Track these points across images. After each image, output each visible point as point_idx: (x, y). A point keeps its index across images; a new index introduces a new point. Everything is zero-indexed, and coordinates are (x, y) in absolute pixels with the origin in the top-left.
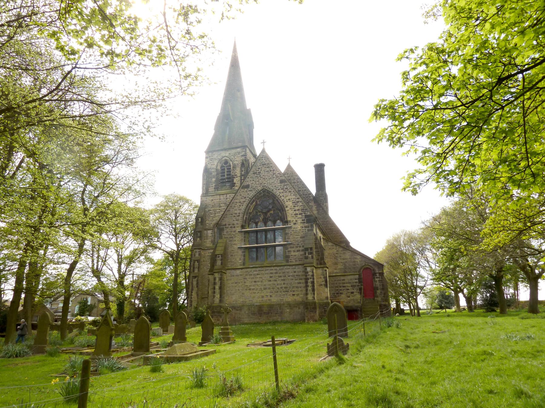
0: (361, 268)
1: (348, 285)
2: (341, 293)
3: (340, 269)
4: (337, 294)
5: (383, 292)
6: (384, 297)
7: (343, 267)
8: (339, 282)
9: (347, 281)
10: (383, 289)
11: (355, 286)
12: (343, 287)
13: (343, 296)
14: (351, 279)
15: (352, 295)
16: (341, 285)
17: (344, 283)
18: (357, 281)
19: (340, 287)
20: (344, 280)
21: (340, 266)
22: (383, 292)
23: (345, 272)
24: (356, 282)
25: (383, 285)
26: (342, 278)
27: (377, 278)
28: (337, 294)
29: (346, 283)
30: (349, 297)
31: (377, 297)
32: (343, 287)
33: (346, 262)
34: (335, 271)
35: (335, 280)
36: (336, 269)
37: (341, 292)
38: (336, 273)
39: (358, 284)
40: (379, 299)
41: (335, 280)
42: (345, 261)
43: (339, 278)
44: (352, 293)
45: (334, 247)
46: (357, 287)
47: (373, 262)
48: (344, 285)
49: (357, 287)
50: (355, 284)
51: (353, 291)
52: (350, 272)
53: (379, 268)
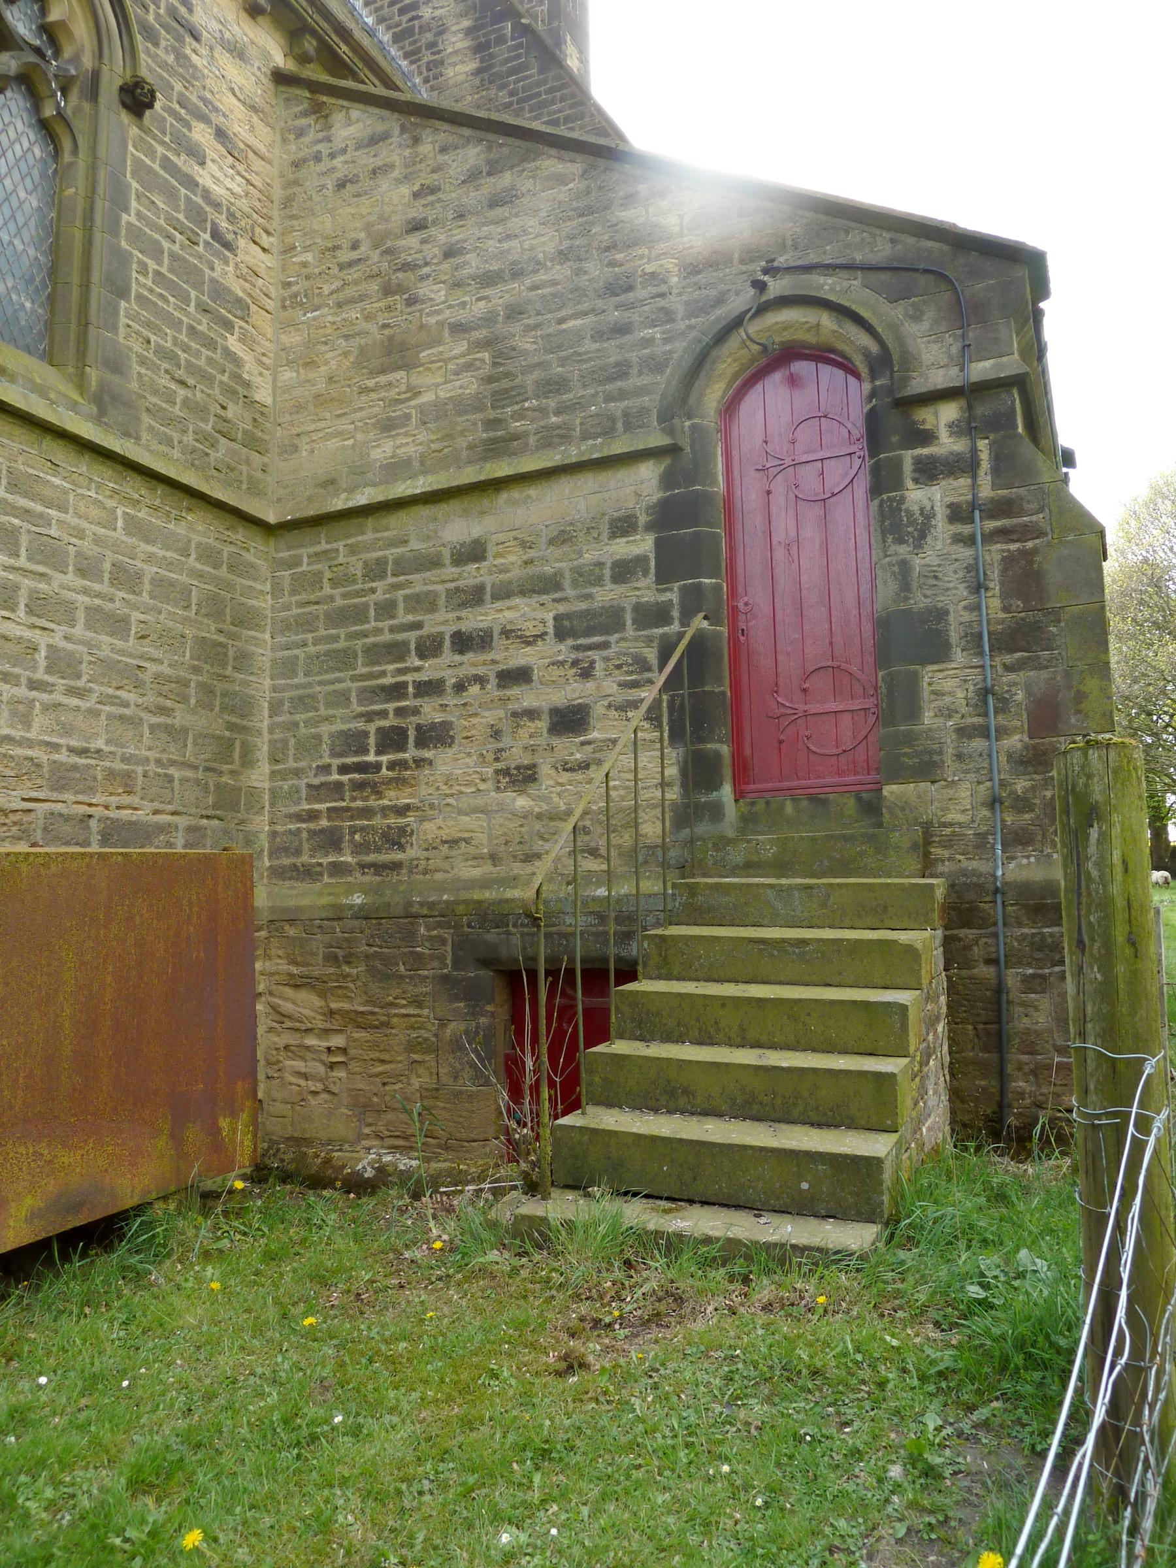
0: (700, 363)
1: (526, 613)
2: (435, 736)
3: (439, 411)
4: (392, 739)
5: (1019, 687)
6: (1035, 760)
7: (469, 385)
8: (419, 583)
9: (508, 562)
10: (1020, 639)
11: (607, 622)
12: (463, 642)
13: (448, 763)
14: (562, 538)
15: (569, 748)
16: (442, 622)
17: (475, 597)
18: (643, 545)
19: (429, 648)
20: (474, 552)
21: (445, 378)
22: (1019, 687)
23: (494, 448)
24: (624, 571)
25: (1025, 579)
26: (457, 527)
27: (928, 471)
28: (392, 739)
29: (503, 593)
30: (523, 777)
31: (927, 769)
32: (463, 642)
33: (514, 312)
34: (383, 451)
35: (376, 571)
36: (388, 426)
37: (430, 711)
38: (396, 468)
39: (645, 590)
40: (957, 801)
41: (376, 571)
42: (499, 297)
43: (415, 532)
44: (570, 720)
45: (394, 153)
46: (631, 641)
47: (882, 249)
48: (474, 620)
49: (631, 641)
50: (607, 594)
51: (573, 692)
52: (547, 442)
53: (964, 315)
